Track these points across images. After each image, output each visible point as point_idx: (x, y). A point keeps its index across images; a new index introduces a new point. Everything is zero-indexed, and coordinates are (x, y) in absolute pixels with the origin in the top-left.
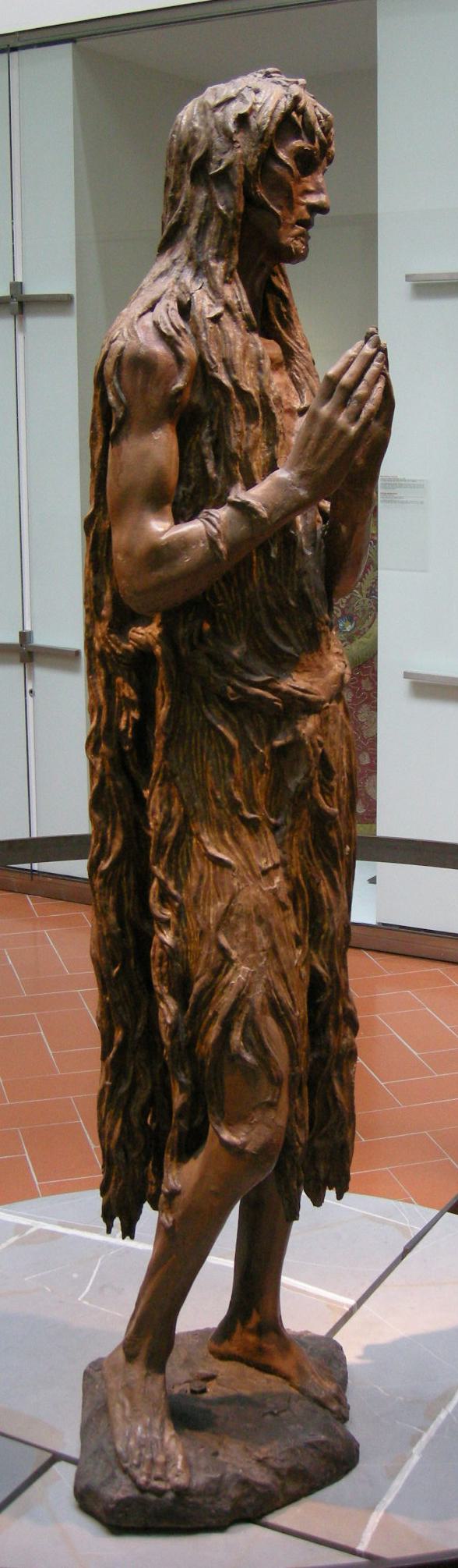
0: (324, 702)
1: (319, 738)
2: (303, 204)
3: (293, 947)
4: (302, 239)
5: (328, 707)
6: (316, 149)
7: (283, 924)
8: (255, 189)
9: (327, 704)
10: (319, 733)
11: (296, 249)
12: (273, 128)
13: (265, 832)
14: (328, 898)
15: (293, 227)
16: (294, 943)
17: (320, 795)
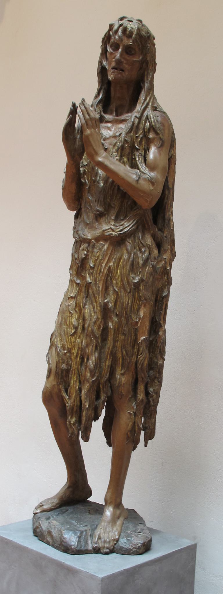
0: (90, 240)
1: (85, 252)
2: (114, 61)
3: (71, 328)
4: (113, 74)
5: (92, 242)
6: (116, 40)
7: (68, 318)
8: (103, 62)
9: (93, 241)
10: (85, 251)
11: (111, 78)
12: (105, 39)
13: (74, 285)
14: (87, 316)
15: (111, 70)
16: (72, 328)
17: (88, 275)
